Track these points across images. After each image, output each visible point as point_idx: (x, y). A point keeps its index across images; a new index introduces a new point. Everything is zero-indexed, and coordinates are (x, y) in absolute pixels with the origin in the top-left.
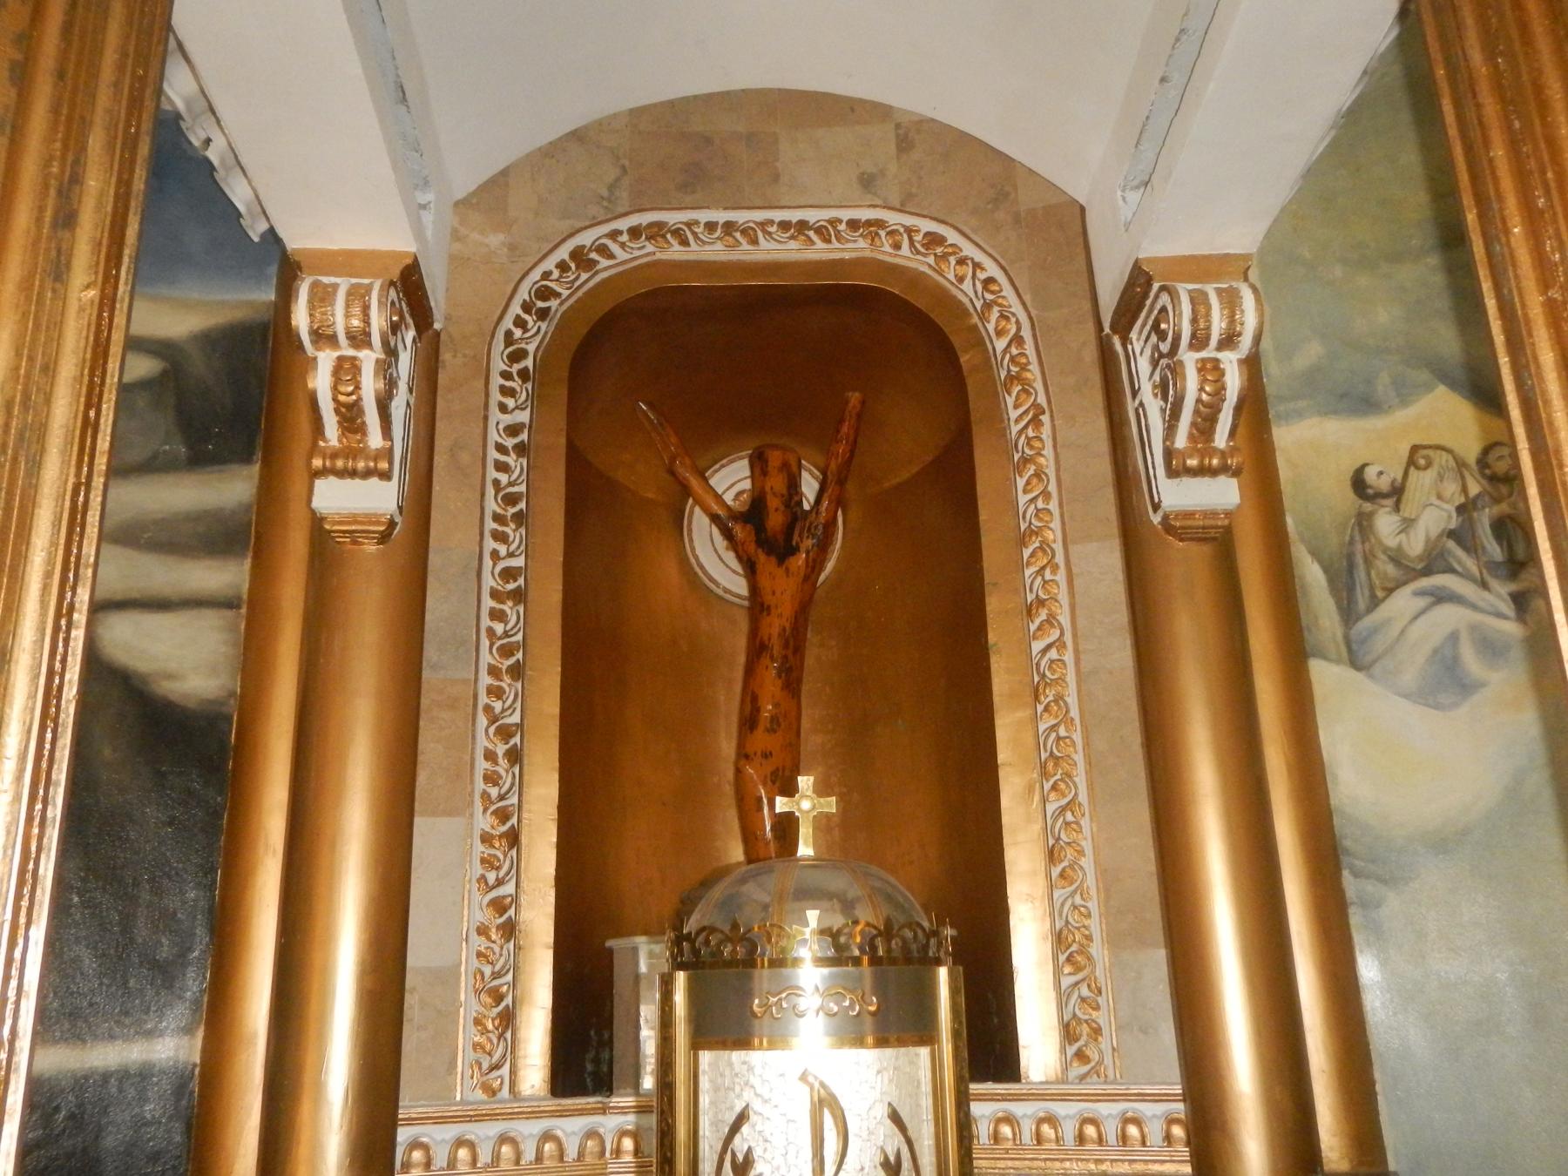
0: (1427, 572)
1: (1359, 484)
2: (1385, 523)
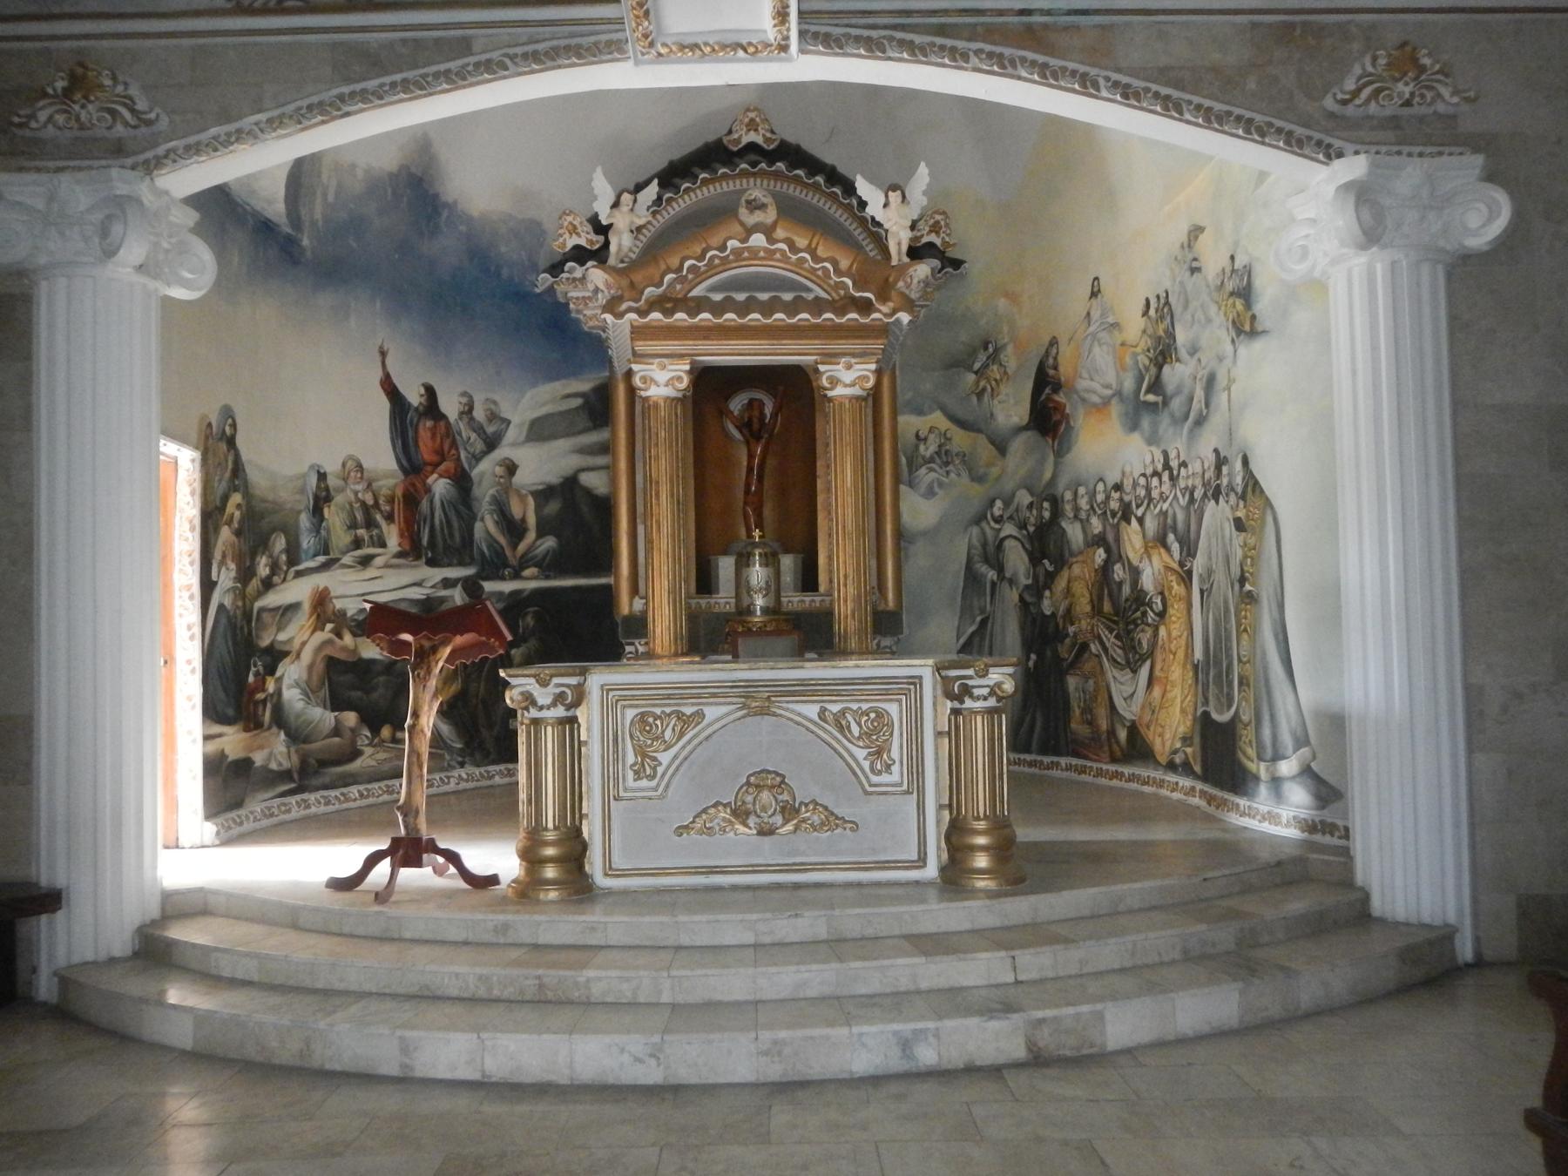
0: (929, 463)
1: (917, 436)
2: (922, 448)
